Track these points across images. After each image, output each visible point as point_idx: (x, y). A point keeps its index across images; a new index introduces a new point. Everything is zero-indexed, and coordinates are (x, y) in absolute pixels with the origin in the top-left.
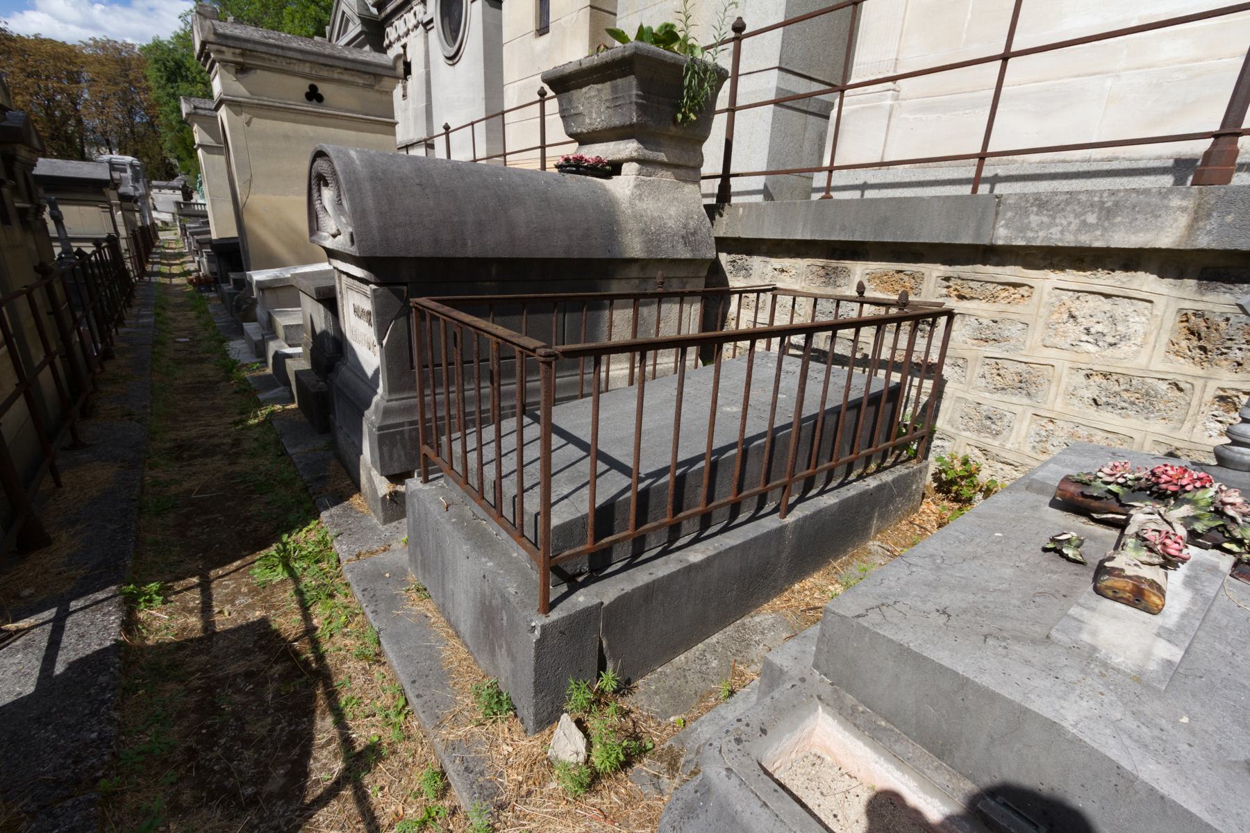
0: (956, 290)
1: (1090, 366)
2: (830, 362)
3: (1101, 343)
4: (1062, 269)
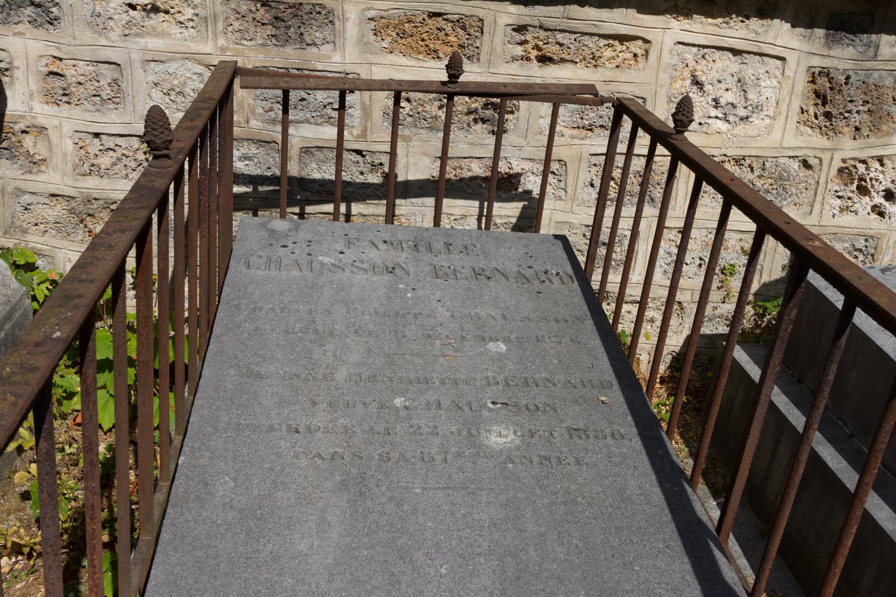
0: (537, 47)
1: (723, 151)
2: (392, 195)
3: (731, 118)
4: (688, 15)
